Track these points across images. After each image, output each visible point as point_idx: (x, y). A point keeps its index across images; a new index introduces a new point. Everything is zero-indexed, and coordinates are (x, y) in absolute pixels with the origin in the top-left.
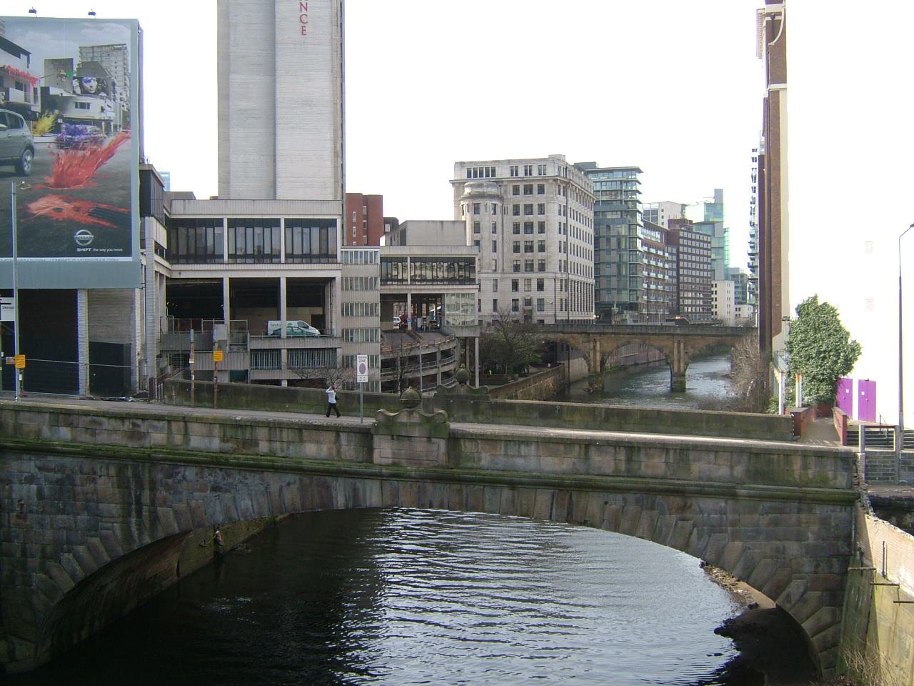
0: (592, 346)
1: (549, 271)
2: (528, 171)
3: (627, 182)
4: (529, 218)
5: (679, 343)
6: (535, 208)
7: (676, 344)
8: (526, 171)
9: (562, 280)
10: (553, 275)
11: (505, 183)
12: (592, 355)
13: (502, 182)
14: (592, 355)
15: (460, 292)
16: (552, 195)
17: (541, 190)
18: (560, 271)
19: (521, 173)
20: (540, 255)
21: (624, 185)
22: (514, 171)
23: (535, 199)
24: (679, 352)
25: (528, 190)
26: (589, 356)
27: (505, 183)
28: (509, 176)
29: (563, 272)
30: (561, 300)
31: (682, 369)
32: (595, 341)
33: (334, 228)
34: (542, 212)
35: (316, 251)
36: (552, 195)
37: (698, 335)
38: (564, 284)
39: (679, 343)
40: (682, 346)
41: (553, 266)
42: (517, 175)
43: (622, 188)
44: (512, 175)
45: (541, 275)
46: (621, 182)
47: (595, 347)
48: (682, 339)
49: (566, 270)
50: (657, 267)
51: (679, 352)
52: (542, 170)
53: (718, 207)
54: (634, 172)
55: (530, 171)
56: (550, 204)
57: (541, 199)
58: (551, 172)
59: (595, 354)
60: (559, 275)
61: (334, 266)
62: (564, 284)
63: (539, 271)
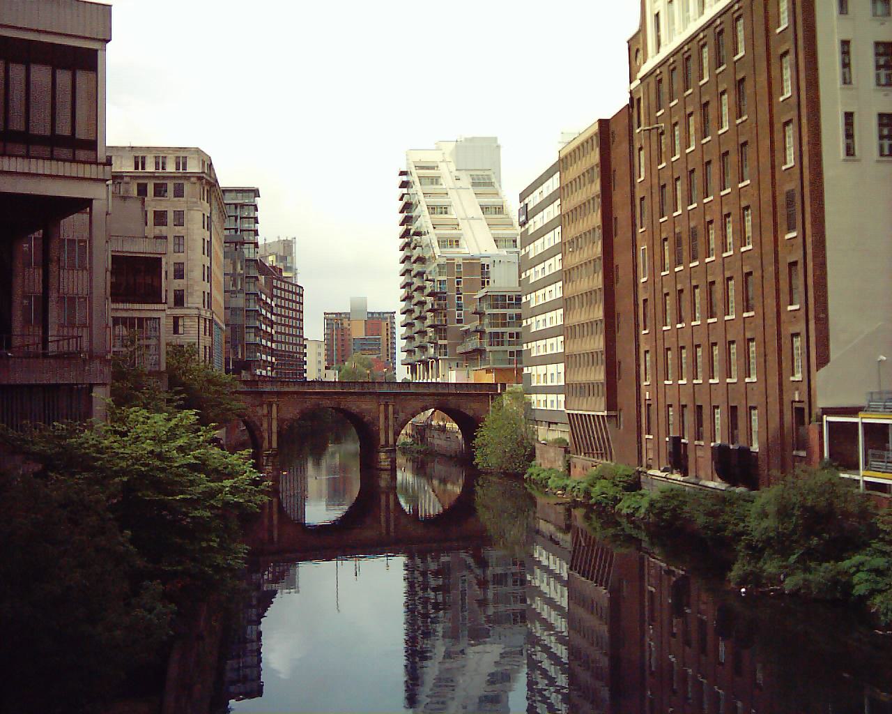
0: (265, 411)
1: (189, 305)
2: (160, 162)
3: (242, 206)
4: (161, 231)
5: (387, 406)
6: (170, 216)
7: (382, 408)
8: (157, 164)
9: (205, 319)
10: (196, 312)
11: (126, 179)
12: (265, 425)
13: (122, 177)
14: (265, 425)
15: (137, 315)
16: (195, 200)
17: (179, 193)
18: (204, 307)
19: (150, 168)
20: (178, 284)
21: (238, 210)
22: (139, 162)
23: (169, 204)
24: (386, 418)
25: (160, 191)
26: (262, 425)
27: (126, 179)
28: (132, 169)
29: (206, 308)
30: (205, 347)
31: (391, 441)
32: (270, 405)
33: (91, 75)
34: (180, 223)
35: (41, 126)
36: (195, 200)
37: (412, 394)
38: (208, 326)
39: (387, 406)
40: (391, 408)
41: (194, 301)
42: (143, 168)
43: (236, 212)
44: (137, 168)
45: (178, 312)
46: (236, 205)
47: (270, 412)
48: (391, 401)
49: (210, 306)
50: (266, 318)
51: (386, 418)
52: (181, 162)
53: (289, 258)
54: (253, 194)
55: (164, 163)
56: (192, 212)
57: (180, 204)
58: (193, 167)
59: (270, 425)
60: (203, 313)
61: (90, 171)
62: (208, 326)
63: (175, 305)
